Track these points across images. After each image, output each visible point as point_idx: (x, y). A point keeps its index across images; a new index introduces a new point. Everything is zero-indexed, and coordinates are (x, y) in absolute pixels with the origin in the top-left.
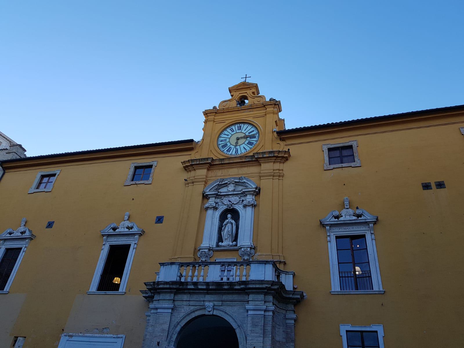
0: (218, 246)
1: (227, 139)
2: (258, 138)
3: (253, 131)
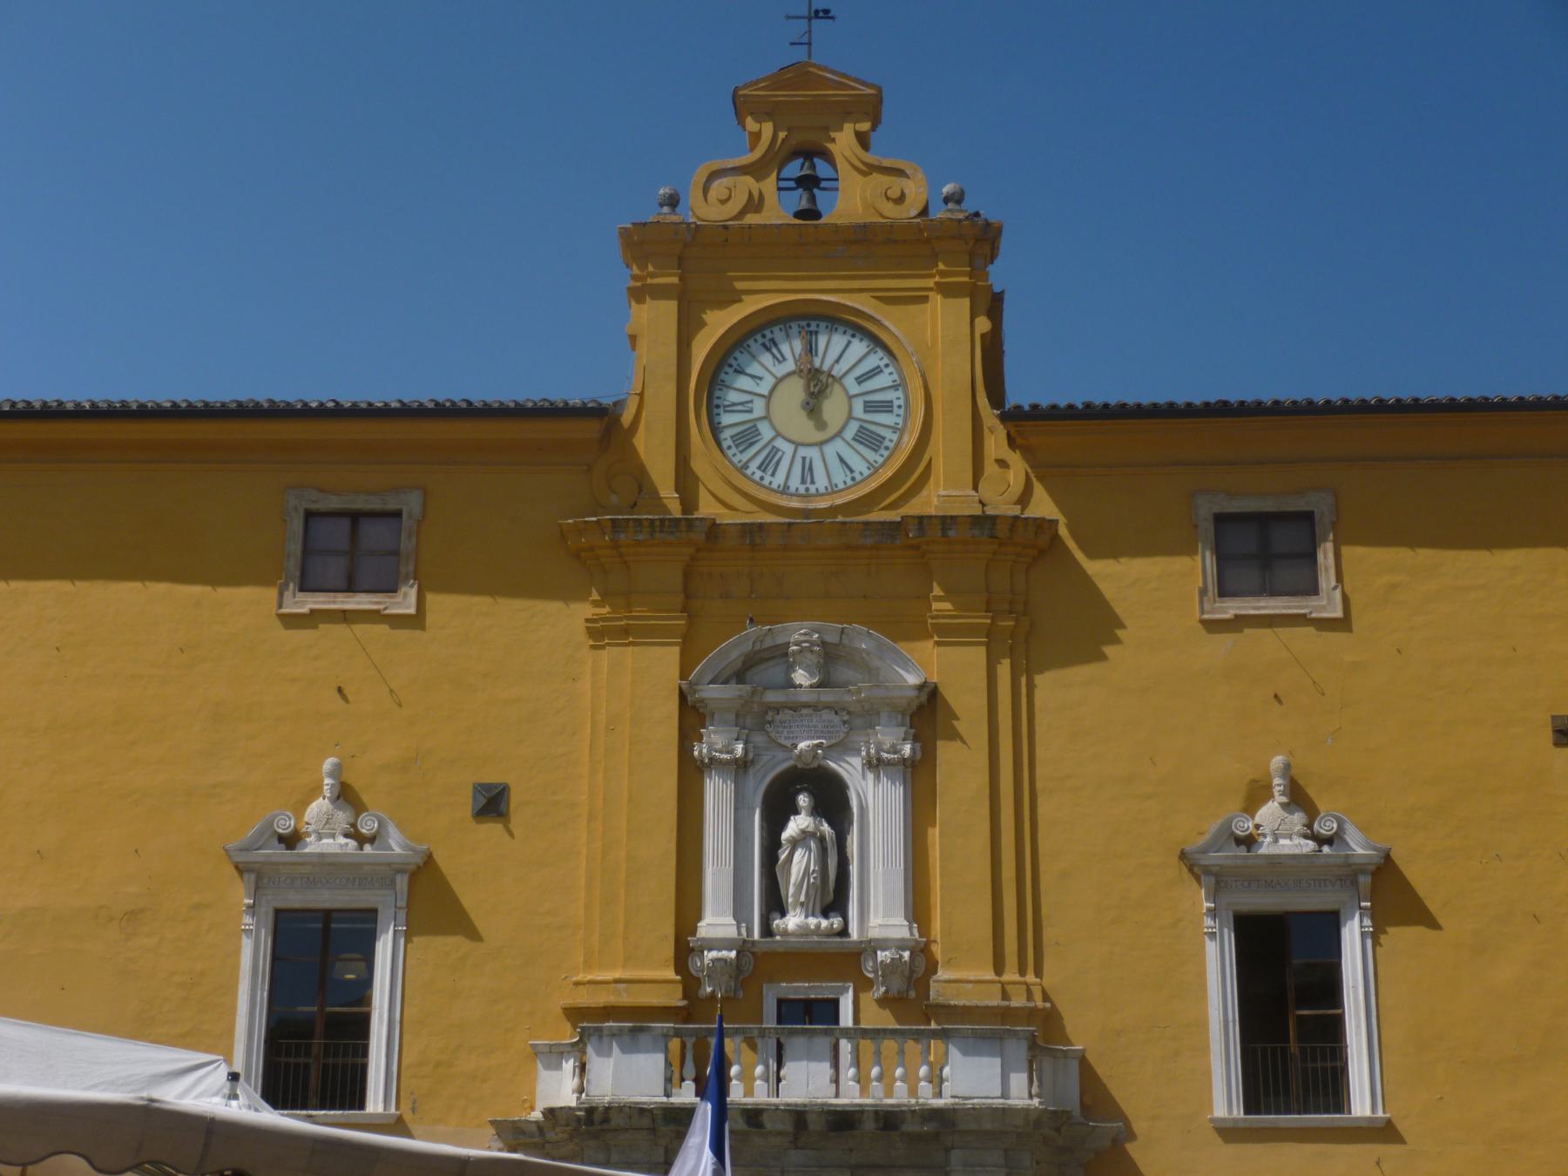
0: (767, 931)
1: (756, 399)
2: (901, 412)
3: (876, 371)
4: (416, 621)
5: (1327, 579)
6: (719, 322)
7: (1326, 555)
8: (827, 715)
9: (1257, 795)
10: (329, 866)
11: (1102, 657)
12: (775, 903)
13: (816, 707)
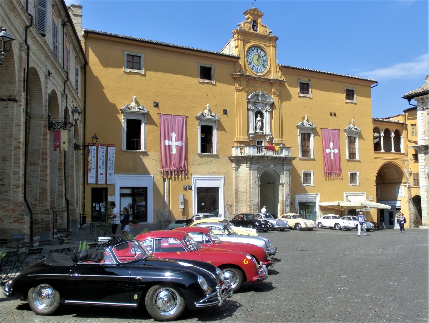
4: (144, 75)
5: (310, 92)
6: (248, 45)
7: (310, 90)
8: (261, 104)
9: (304, 118)
10: (209, 120)
11: (290, 100)
12: (256, 129)
13: (261, 103)
